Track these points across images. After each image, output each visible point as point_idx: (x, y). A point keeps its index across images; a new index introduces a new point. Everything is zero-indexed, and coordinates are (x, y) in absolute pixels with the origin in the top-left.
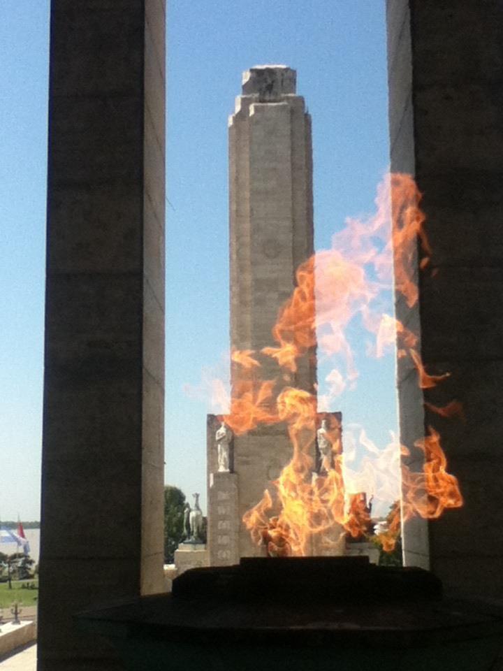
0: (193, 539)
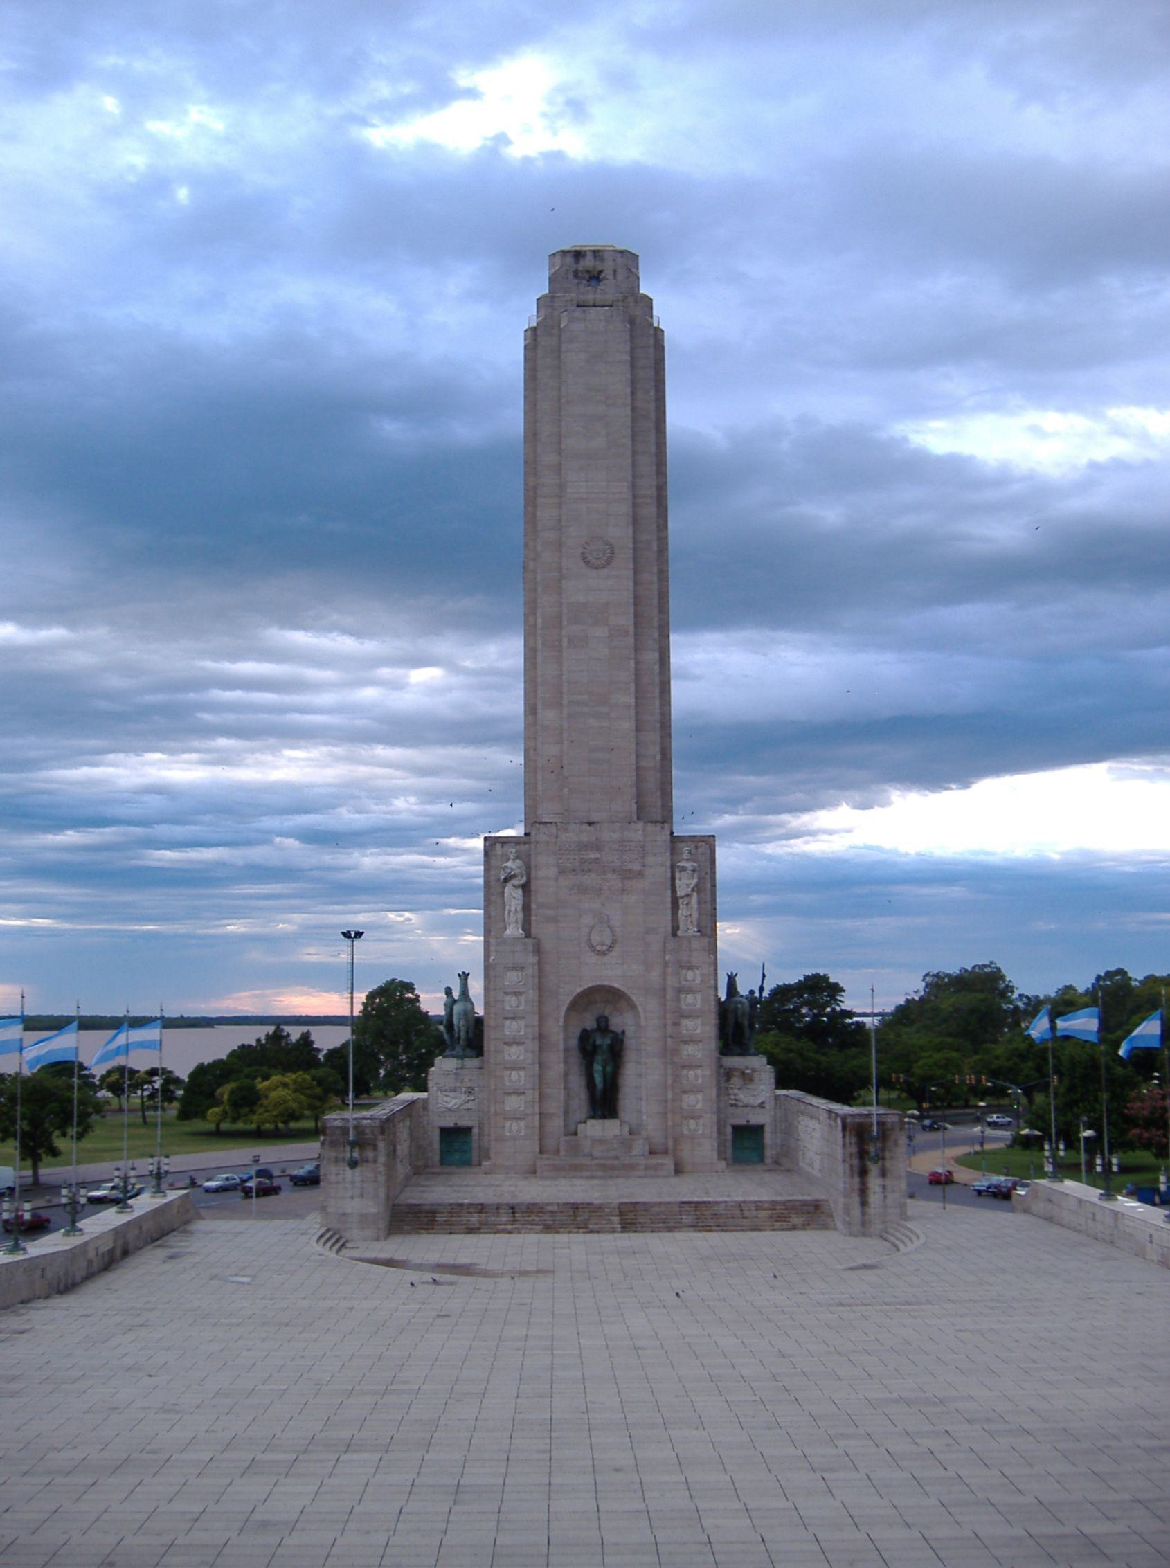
0: (458, 1050)
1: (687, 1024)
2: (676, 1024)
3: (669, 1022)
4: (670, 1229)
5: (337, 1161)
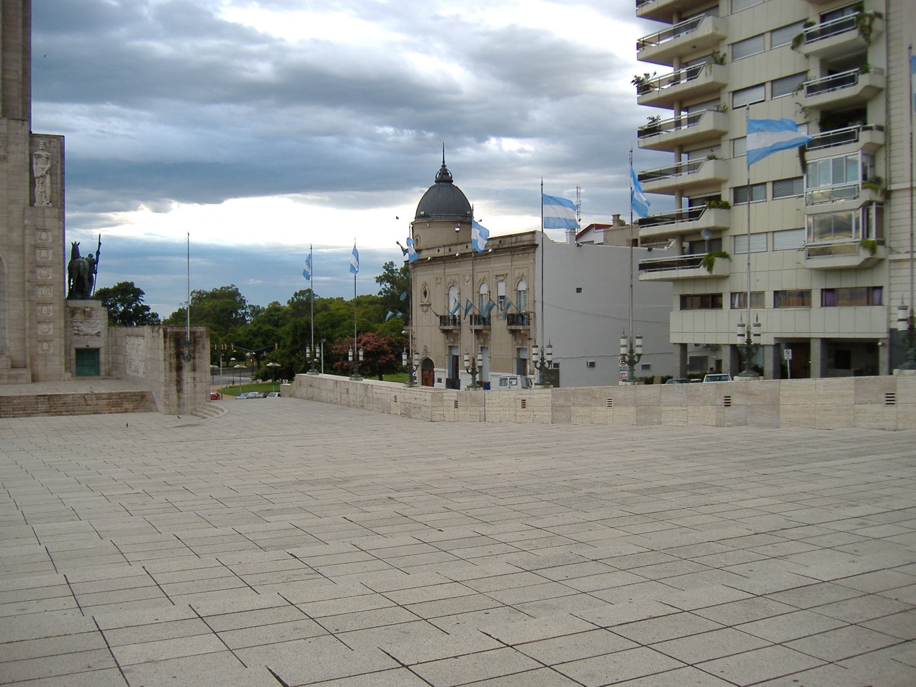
1: (42, 272)
2: (33, 272)
3: (27, 270)
4: (29, 415)
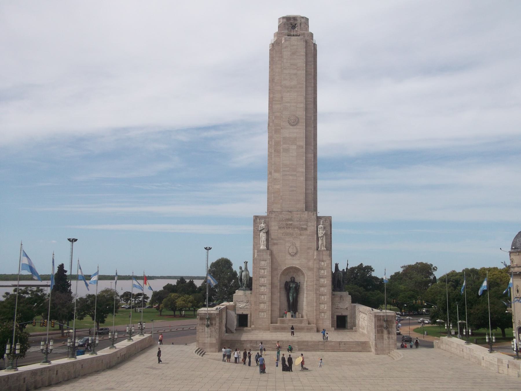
0: (244, 288)
5: (203, 324)
